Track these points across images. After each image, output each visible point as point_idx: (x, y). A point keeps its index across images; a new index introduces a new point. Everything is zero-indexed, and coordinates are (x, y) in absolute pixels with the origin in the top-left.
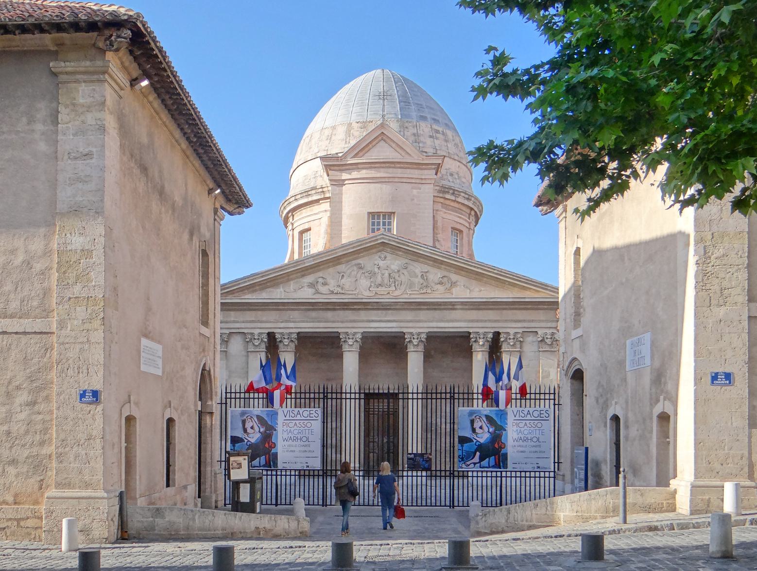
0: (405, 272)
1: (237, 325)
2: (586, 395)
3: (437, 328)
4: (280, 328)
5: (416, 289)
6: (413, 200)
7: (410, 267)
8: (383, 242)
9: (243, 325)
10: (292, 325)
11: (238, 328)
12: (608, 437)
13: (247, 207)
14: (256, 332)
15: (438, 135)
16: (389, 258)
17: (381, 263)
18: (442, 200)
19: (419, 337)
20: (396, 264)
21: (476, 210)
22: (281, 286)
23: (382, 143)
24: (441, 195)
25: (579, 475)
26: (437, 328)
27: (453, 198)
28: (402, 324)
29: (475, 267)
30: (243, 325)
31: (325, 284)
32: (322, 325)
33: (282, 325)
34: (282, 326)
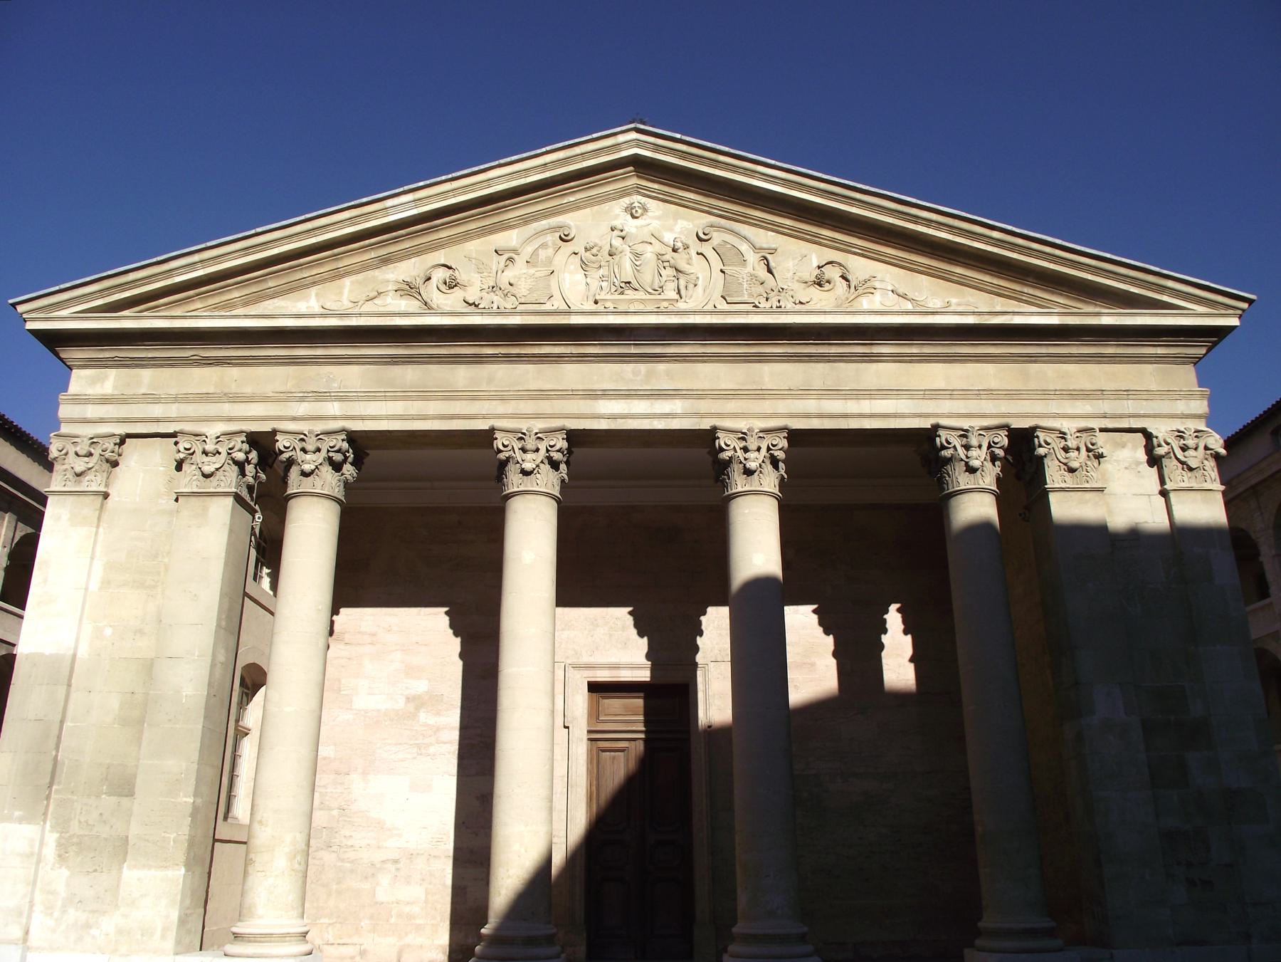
0: (706, 249)
1: (157, 410)
3: (820, 416)
4: (294, 419)
5: (746, 298)
7: (717, 237)
9: (173, 410)
10: (334, 408)
11: (157, 420)
14: (213, 430)
16: (658, 213)
17: (631, 226)
20: (678, 228)
22: (313, 291)
26: (820, 416)
28: (705, 406)
29: (928, 223)
30: (173, 410)
31: (452, 285)
32: (434, 407)
33: (303, 409)
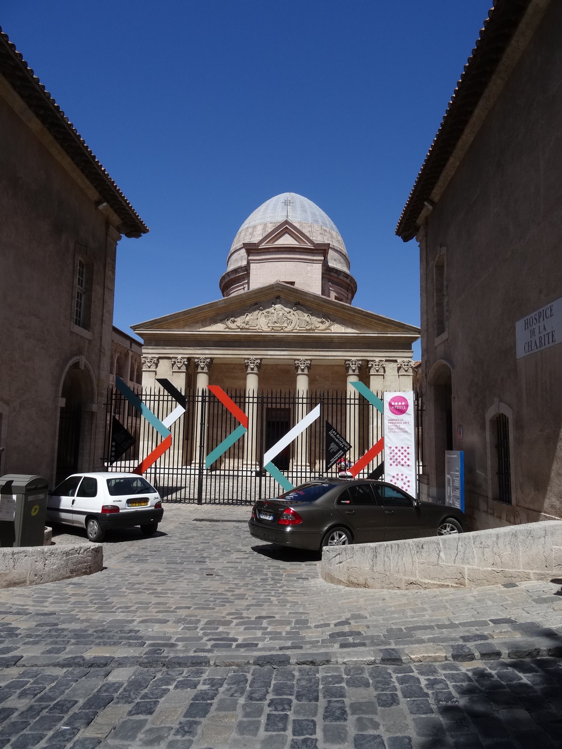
2: (454, 398)
6: (308, 274)
8: (278, 290)
12: (488, 440)
13: (144, 232)
15: (326, 234)
18: (328, 277)
19: (305, 363)
21: (352, 286)
23: (287, 235)
24: (328, 273)
25: (453, 483)
27: (336, 276)
34: (199, 353)
